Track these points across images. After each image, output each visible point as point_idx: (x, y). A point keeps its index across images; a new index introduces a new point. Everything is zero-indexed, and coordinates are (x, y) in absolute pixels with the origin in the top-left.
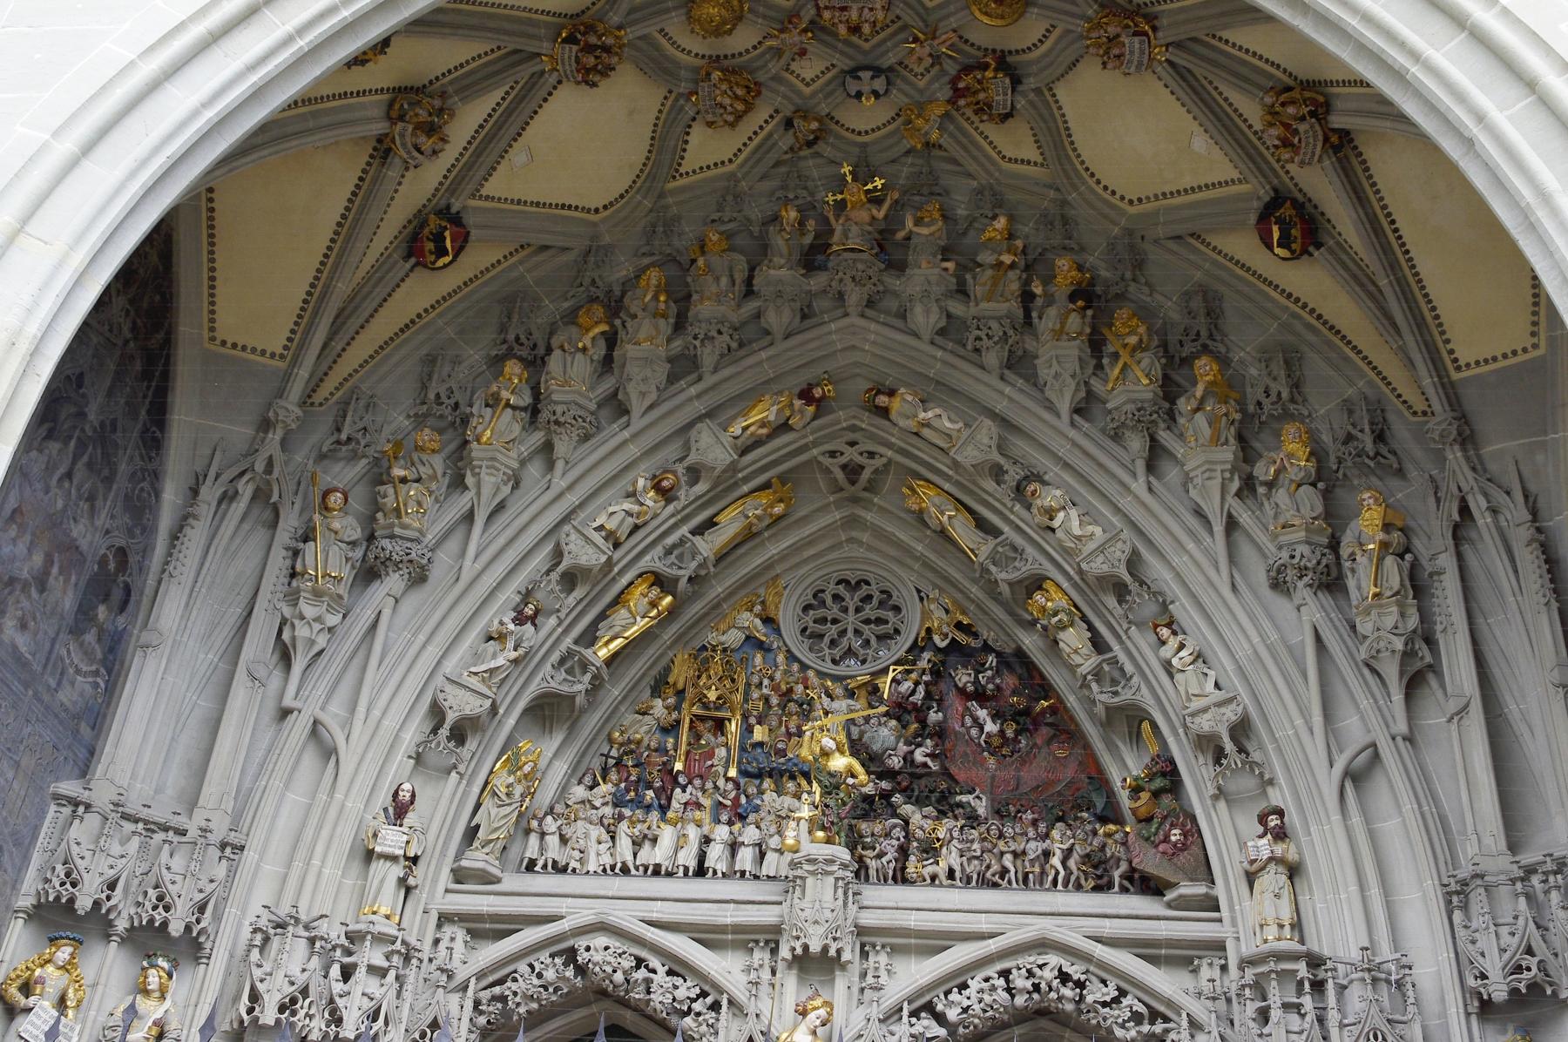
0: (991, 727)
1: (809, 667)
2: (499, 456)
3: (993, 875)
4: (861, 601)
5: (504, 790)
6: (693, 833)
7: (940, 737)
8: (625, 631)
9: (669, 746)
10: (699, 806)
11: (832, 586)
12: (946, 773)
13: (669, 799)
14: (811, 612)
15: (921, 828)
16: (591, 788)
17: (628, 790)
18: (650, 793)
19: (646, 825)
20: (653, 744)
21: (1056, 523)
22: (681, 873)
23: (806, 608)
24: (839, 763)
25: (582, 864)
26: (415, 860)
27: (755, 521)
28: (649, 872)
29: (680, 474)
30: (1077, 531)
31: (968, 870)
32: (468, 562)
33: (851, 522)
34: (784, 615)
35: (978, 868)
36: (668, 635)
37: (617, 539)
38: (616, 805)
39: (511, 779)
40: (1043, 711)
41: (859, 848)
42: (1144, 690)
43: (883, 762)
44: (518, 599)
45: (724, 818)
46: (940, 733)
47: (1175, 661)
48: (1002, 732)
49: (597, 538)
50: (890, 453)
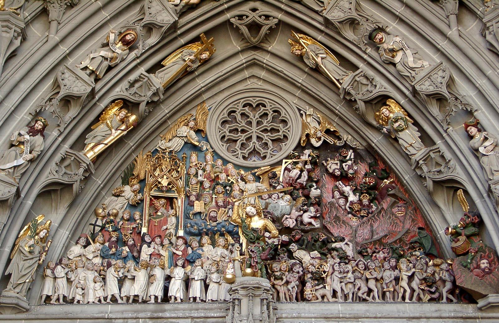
0: (352, 198)
2: (12, 20)
3: (363, 294)
5: (27, 249)
6: (159, 273)
7: (319, 205)
9: (137, 217)
10: (160, 255)
11: (240, 107)
12: (324, 227)
13: (139, 252)
14: (228, 126)
15: (312, 265)
16: (85, 247)
17: (110, 248)
18: (127, 249)
19: (126, 270)
20: (126, 216)
21: (397, 59)
22: (153, 301)
23: (224, 122)
24: (257, 223)
25: (83, 297)
27: (190, 64)
28: (131, 301)
30: (411, 65)
31: (346, 292)
33: (253, 64)
34: (210, 127)
35: (352, 291)
36: (131, 143)
37: (97, 76)
38: (103, 258)
40: (387, 188)
41: (272, 279)
42: (459, 169)
43: (282, 224)
44: (29, 118)
45: (180, 263)
46: (319, 202)
47: (481, 150)
48: (360, 200)
49: (84, 75)
50: (280, 16)
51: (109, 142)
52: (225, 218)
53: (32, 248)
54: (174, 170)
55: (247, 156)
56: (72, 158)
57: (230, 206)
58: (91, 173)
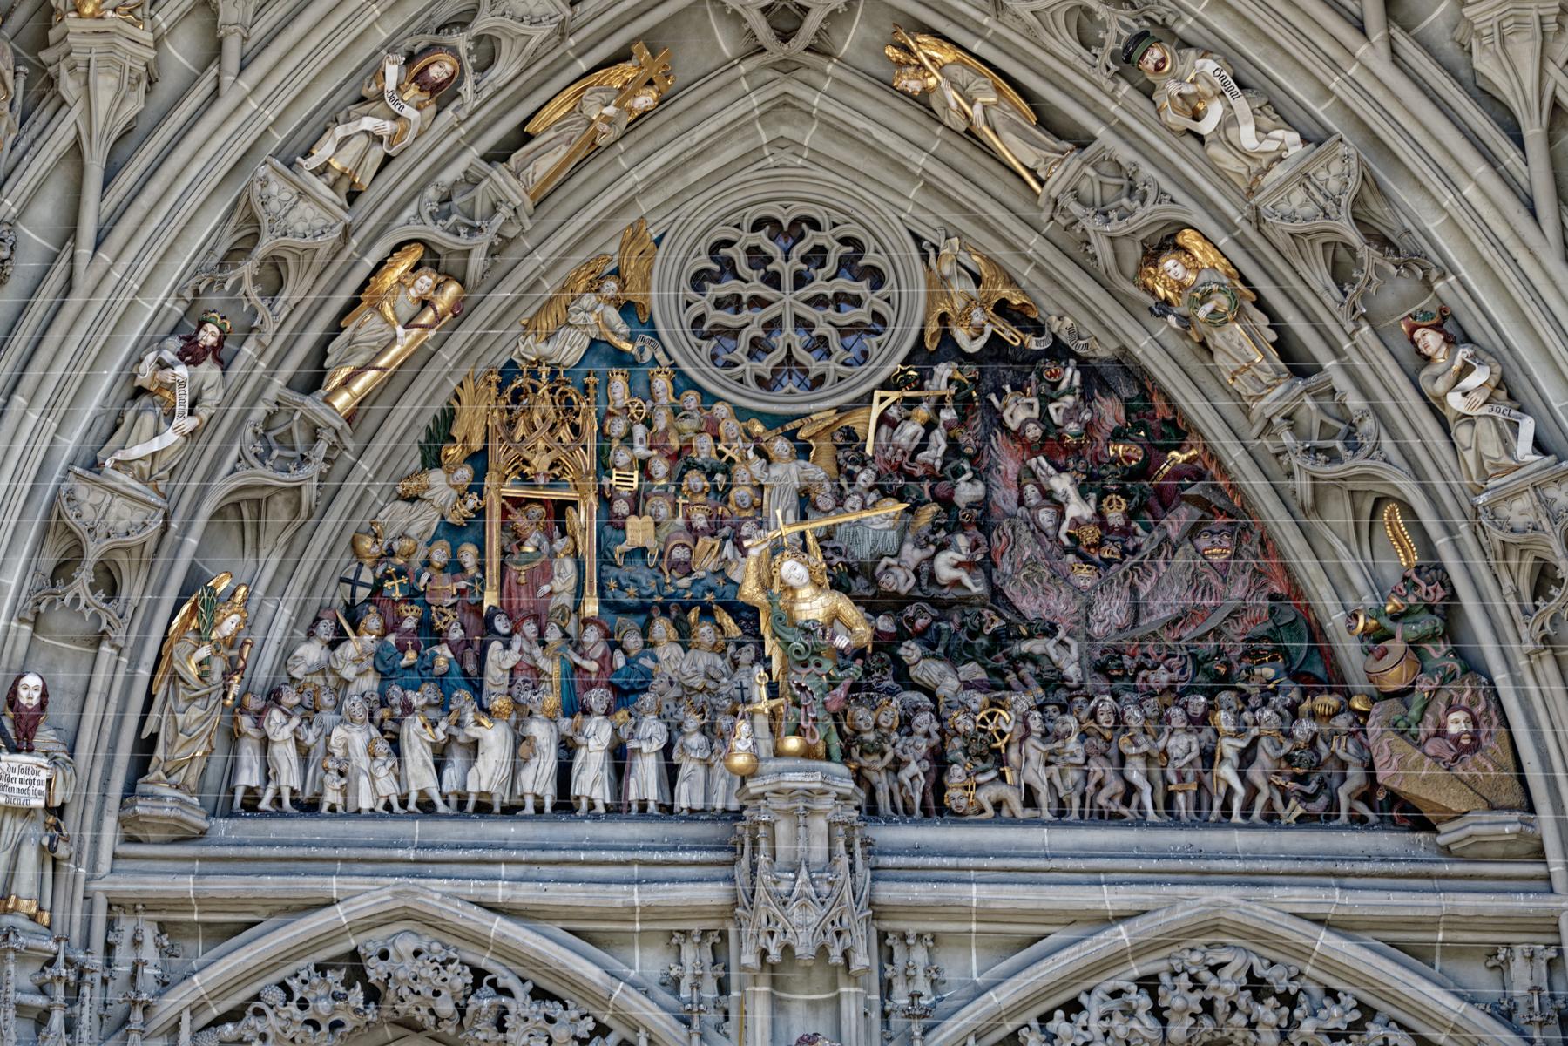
1: (717, 399)
4: (804, 259)
5: (193, 669)
8: (379, 355)
10: (537, 672)
13: (481, 659)
26: (60, 811)
29: (463, 53)
32: (85, 251)
33: (783, 105)
39: (204, 652)
49: (320, 186)
51: (392, 363)
52: (711, 563)
53: (206, 668)
54: (563, 423)
55: (768, 377)
56: (297, 417)
57: (725, 531)
58: (345, 449)
